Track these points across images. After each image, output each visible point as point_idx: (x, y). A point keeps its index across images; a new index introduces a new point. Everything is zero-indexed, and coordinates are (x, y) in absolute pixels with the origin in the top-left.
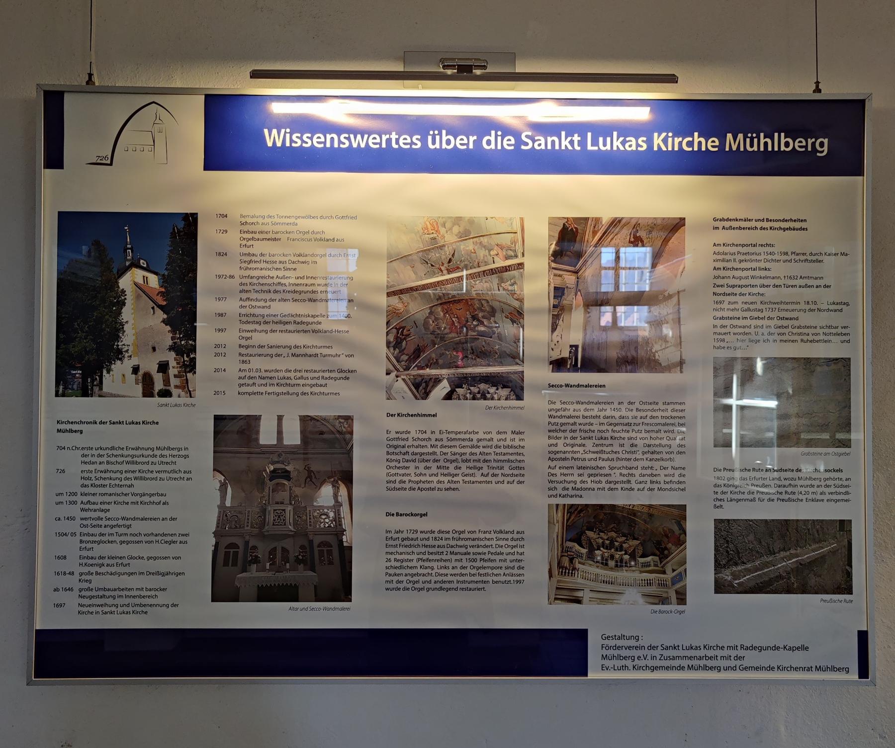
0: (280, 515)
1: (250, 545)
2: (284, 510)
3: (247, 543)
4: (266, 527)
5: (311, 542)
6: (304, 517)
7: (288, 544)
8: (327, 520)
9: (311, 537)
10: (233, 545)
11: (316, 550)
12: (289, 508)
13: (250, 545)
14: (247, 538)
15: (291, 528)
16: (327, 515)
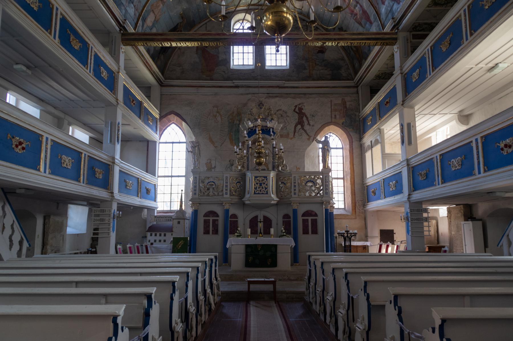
0: (262, 185)
1: (230, 213)
2: (266, 177)
3: (227, 211)
4: (247, 196)
5: (295, 212)
6: (288, 185)
7: (271, 214)
8: (313, 188)
9: (295, 207)
10: (213, 213)
11: (300, 219)
12: (272, 174)
13: (230, 213)
14: (227, 207)
15: (274, 196)
16: (314, 183)
